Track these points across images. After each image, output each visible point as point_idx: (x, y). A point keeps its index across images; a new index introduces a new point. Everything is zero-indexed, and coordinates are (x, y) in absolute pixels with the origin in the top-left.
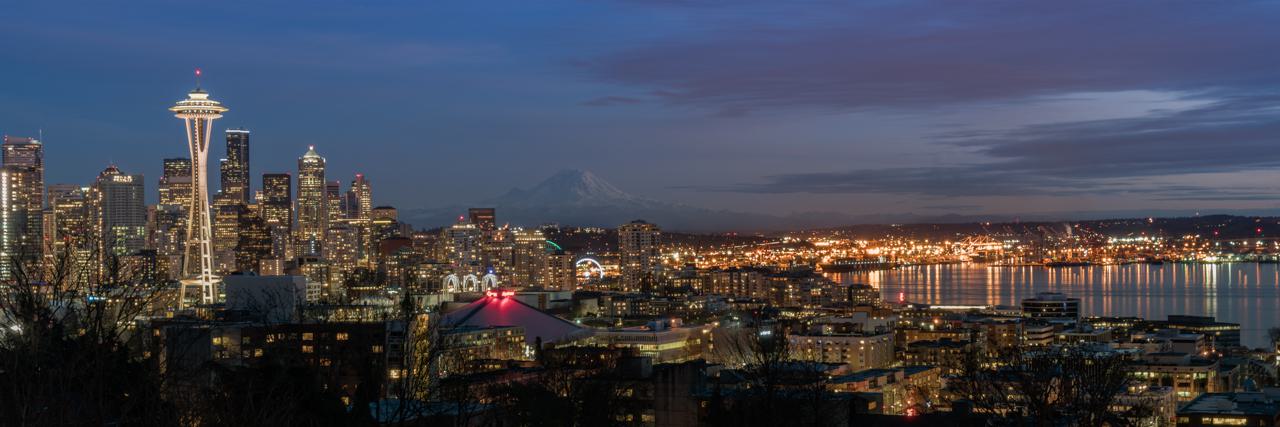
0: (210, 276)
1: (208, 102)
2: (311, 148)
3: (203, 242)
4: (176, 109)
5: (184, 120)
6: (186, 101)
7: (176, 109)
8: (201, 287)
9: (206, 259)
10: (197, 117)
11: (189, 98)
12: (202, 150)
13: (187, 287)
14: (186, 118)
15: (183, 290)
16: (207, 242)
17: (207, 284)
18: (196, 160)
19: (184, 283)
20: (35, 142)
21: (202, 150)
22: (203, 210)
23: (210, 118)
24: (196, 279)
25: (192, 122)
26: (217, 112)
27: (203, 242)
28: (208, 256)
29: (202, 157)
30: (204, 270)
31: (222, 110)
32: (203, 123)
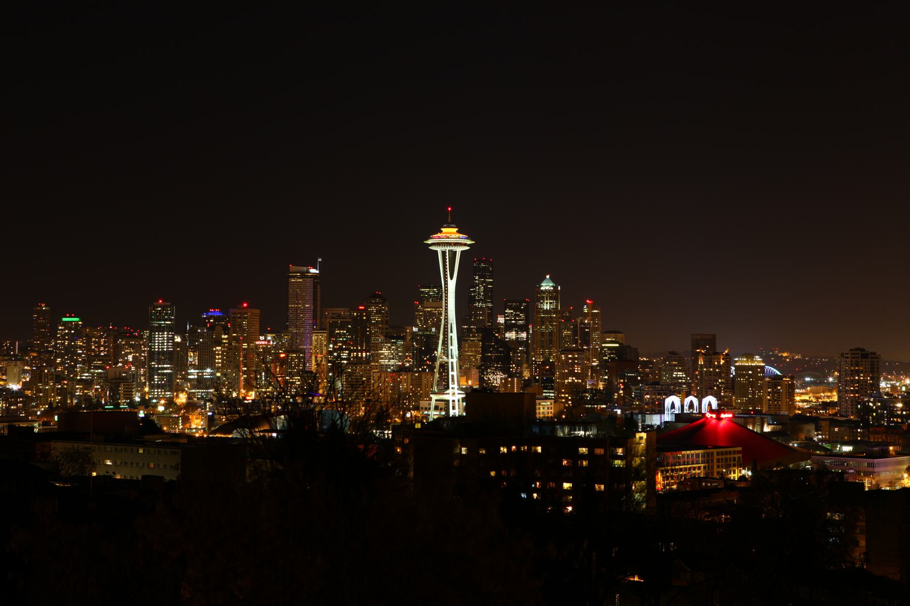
0: (457, 391)
1: (458, 235)
2: (548, 277)
4: (430, 242)
6: (439, 235)
7: (430, 242)
8: (447, 401)
9: (453, 376)
10: (447, 249)
11: (441, 232)
12: (451, 278)
13: (436, 400)
14: (439, 249)
15: (433, 403)
16: (455, 360)
17: (453, 398)
18: (446, 287)
19: (434, 397)
21: (451, 278)
22: (451, 332)
23: (459, 250)
24: (444, 394)
25: (444, 253)
26: (465, 245)
28: (455, 373)
29: (452, 284)
30: (451, 386)
31: (469, 242)
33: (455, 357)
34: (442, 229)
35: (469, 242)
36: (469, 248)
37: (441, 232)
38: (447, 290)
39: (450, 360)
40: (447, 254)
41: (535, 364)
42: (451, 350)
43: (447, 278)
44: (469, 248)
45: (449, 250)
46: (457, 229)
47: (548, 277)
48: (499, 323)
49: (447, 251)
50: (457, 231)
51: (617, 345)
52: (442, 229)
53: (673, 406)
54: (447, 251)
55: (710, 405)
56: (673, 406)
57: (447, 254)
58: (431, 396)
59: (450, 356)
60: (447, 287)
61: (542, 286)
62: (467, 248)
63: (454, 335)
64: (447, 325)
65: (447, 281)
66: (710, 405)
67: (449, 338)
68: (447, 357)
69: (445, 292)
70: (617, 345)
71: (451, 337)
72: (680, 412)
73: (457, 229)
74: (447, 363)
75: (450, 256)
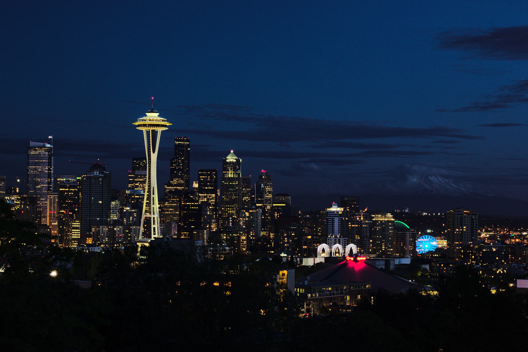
1: (159, 118)
2: (232, 152)
3: (154, 216)
4: (137, 124)
5: (143, 131)
6: (144, 118)
7: (137, 124)
9: (154, 228)
10: (151, 129)
11: (146, 116)
12: (154, 152)
14: (144, 129)
16: (156, 216)
20: (48, 146)
21: (154, 152)
22: (153, 194)
23: (160, 130)
25: (148, 132)
26: (165, 126)
27: (154, 216)
28: (156, 226)
29: (154, 157)
31: (168, 124)
32: (155, 133)
33: (156, 213)
34: (146, 114)
35: (168, 124)
36: (168, 129)
37: (146, 116)
38: (150, 162)
39: (152, 216)
40: (151, 133)
41: (221, 220)
42: (153, 207)
43: (150, 152)
44: (168, 129)
45: (152, 130)
46: (158, 114)
47: (232, 152)
48: (194, 187)
49: (151, 131)
50: (159, 116)
51: (285, 205)
52: (146, 114)
53: (323, 251)
54: (151, 131)
55: (351, 250)
56: (323, 251)
57: (151, 133)
58: (138, 244)
59: (152, 213)
60: (150, 159)
61: (227, 159)
62: (166, 129)
63: (156, 196)
64: (150, 189)
65: (150, 154)
66: (351, 250)
67: (152, 199)
68: (150, 213)
69: (149, 163)
70: (285, 205)
71: (153, 197)
72: (329, 256)
73: (158, 114)
74: (150, 218)
75: (153, 135)
